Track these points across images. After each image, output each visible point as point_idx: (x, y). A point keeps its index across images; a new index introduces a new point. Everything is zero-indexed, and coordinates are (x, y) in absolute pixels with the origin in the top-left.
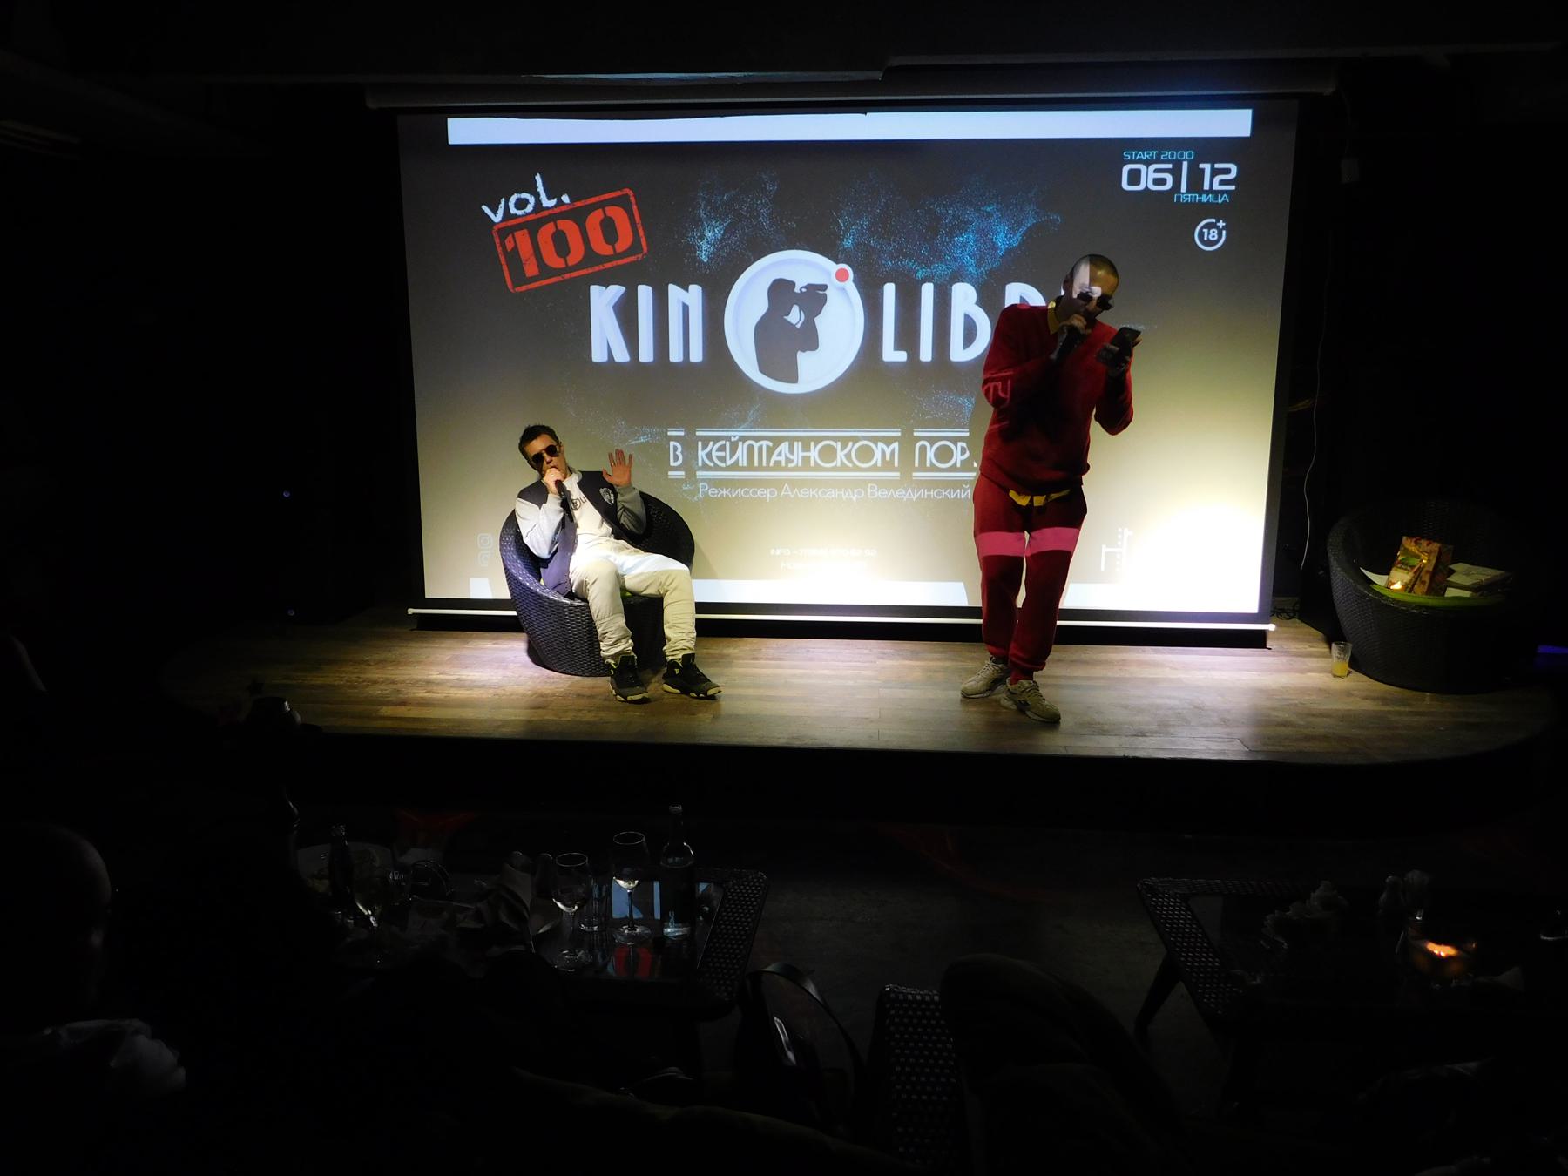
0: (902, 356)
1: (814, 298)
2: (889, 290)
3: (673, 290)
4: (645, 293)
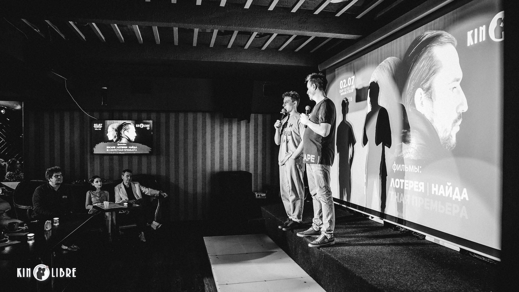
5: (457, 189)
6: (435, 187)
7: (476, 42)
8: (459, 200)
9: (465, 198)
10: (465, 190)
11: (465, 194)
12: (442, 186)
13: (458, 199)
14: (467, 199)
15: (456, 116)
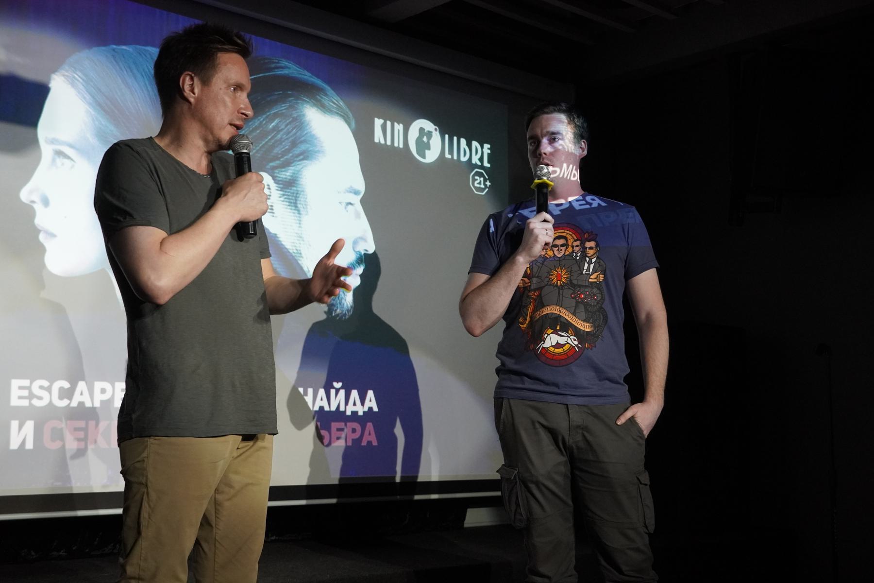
0: (450, 157)
1: (429, 135)
2: (447, 136)
3: (396, 124)
4: (389, 123)
5: (355, 394)
7: (389, 143)
8: (361, 413)
9: (370, 409)
10: (370, 394)
13: (357, 412)
14: (376, 409)
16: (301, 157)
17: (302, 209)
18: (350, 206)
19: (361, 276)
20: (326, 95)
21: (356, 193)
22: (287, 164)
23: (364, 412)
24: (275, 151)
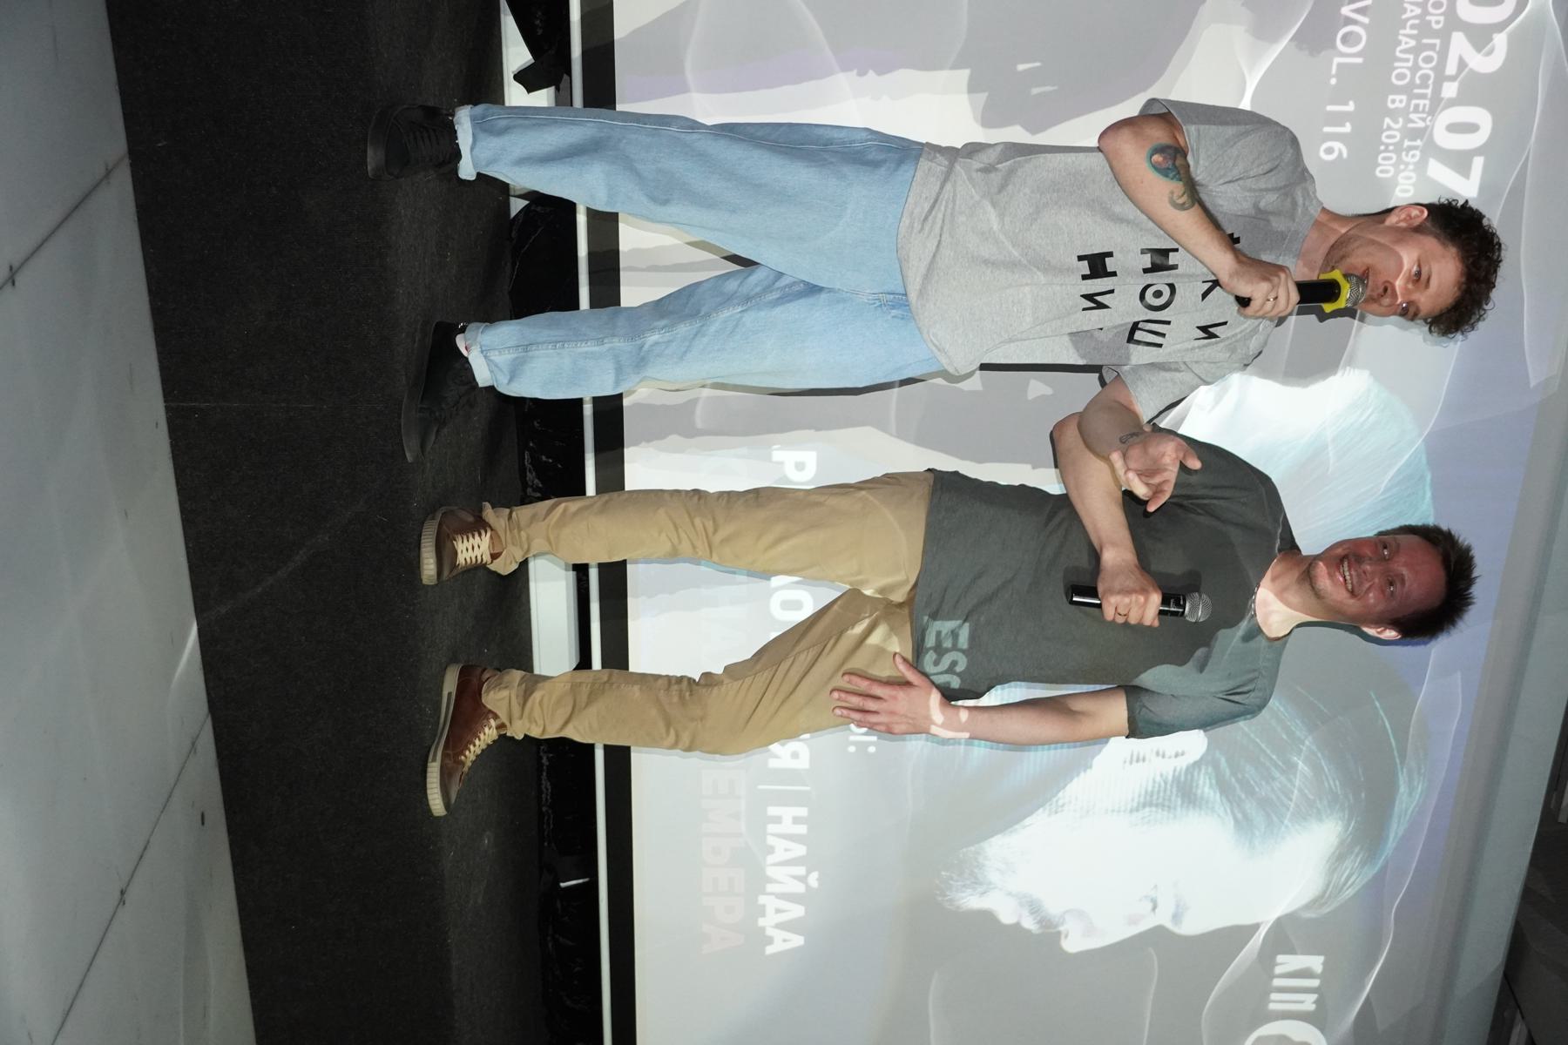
5: (797, 911)
6: (797, 820)
8: (761, 922)
9: (770, 941)
10: (797, 941)
11: (784, 942)
12: (800, 850)
13: (763, 915)
14: (770, 950)
15: (1053, 908)
16: (1239, 816)
17: (1140, 814)
18: (1150, 906)
19: (1017, 926)
20: (1363, 864)
21: (1176, 917)
22: (1224, 788)
23: (763, 929)
24: (1248, 768)
